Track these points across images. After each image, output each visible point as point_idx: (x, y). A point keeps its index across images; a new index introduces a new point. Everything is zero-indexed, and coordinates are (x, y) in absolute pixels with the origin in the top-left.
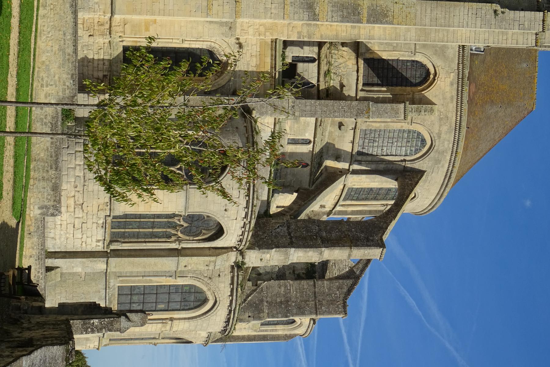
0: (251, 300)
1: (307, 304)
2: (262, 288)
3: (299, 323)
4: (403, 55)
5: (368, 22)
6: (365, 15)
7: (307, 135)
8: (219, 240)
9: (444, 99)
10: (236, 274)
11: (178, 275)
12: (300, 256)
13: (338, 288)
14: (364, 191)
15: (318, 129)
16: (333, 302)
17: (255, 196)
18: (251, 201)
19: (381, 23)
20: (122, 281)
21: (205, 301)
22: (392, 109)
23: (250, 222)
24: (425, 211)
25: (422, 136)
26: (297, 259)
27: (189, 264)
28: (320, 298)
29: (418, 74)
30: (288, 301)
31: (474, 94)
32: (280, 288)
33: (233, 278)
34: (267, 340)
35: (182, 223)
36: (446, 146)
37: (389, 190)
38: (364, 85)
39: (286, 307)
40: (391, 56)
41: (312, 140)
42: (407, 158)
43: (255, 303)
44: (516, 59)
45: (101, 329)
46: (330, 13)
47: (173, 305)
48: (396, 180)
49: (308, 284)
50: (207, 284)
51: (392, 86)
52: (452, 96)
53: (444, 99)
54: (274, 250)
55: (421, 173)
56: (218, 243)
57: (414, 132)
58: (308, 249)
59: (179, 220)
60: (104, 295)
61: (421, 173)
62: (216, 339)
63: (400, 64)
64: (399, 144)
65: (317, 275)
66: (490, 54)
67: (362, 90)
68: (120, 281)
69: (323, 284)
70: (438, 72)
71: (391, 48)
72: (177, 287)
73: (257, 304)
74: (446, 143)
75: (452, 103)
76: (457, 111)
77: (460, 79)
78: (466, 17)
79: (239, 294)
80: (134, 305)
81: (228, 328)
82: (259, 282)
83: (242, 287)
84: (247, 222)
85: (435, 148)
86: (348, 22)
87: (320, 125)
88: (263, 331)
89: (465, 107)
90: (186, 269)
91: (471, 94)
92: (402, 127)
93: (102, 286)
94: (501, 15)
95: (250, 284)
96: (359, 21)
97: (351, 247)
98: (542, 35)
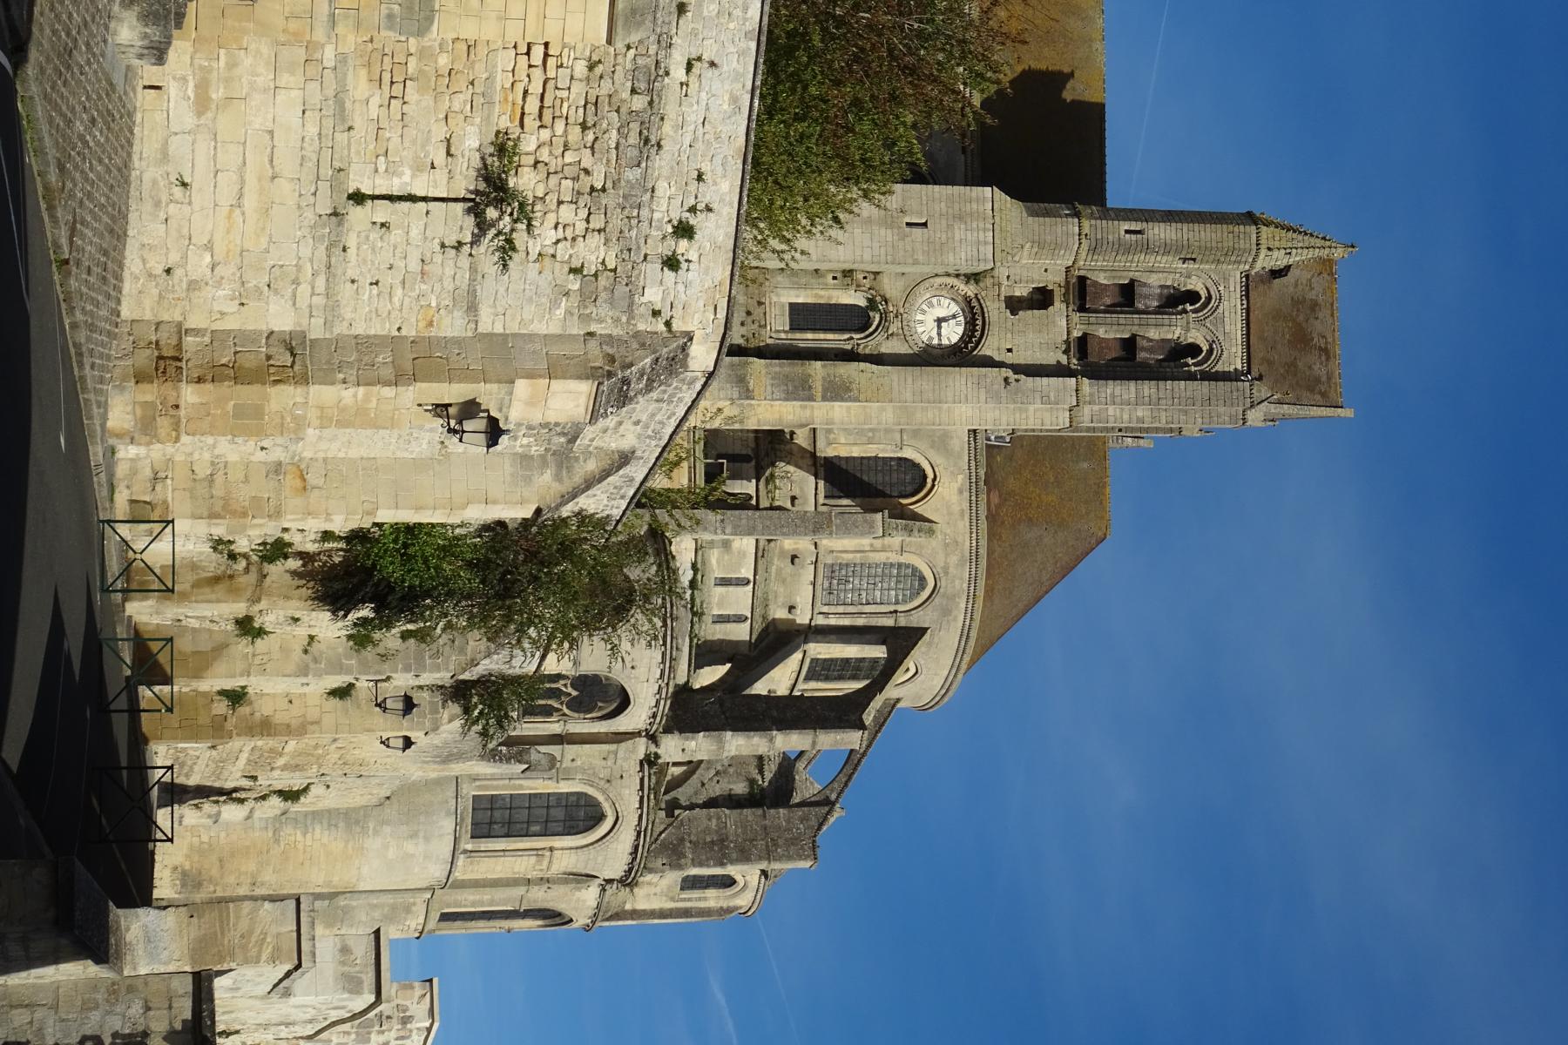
0: (665, 839)
1: (754, 846)
2: (682, 820)
3: (742, 884)
4: (883, 450)
5: (824, 399)
6: (820, 389)
7: (743, 571)
8: (622, 715)
9: (950, 514)
10: (646, 774)
11: (561, 776)
12: (741, 745)
13: (803, 819)
14: (835, 666)
15: (760, 562)
16: (793, 841)
17: (674, 645)
18: (668, 652)
19: (843, 400)
20: (480, 788)
21: (601, 817)
22: (866, 521)
23: (667, 684)
24: (937, 699)
25: (920, 572)
26: (737, 749)
27: (577, 756)
28: (775, 835)
29: (908, 478)
30: (722, 841)
31: (999, 506)
32: (709, 820)
33: (642, 780)
34: (692, 916)
35: (570, 690)
36: (958, 587)
37: (875, 661)
38: (826, 497)
39: (721, 849)
40: (865, 451)
41: (752, 578)
42: (900, 608)
43: (672, 843)
44: (1069, 455)
45: (510, 759)
46: (769, 388)
47: (553, 826)
48: (883, 643)
49: (754, 813)
50: (604, 792)
51: (869, 497)
52: (963, 510)
53: (950, 514)
54: (701, 734)
55: (922, 631)
56: (623, 723)
57: (907, 566)
58: (752, 733)
59: (565, 685)
60: (454, 807)
61: (922, 631)
62: (610, 914)
63: (880, 463)
64: (885, 585)
65: (767, 801)
66: (1022, 446)
67: (824, 505)
68: (479, 786)
69: (778, 813)
70: (938, 474)
71: (864, 439)
72: (559, 796)
73: (674, 845)
75: (963, 519)
76: (971, 533)
77: (973, 486)
78: (964, 387)
79: (651, 804)
80: (495, 826)
81: (635, 863)
82: (677, 812)
83: (655, 793)
84: (663, 685)
85: (942, 590)
86: (795, 400)
87: (763, 556)
88: (684, 900)
89: (984, 525)
90: (574, 764)
91: (993, 506)
92: (888, 558)
93: (451, 793)
94: (1014, 383)
95: (662, 814)
96: (811, 398)
97: (815, 729)
98: (1079, 411)
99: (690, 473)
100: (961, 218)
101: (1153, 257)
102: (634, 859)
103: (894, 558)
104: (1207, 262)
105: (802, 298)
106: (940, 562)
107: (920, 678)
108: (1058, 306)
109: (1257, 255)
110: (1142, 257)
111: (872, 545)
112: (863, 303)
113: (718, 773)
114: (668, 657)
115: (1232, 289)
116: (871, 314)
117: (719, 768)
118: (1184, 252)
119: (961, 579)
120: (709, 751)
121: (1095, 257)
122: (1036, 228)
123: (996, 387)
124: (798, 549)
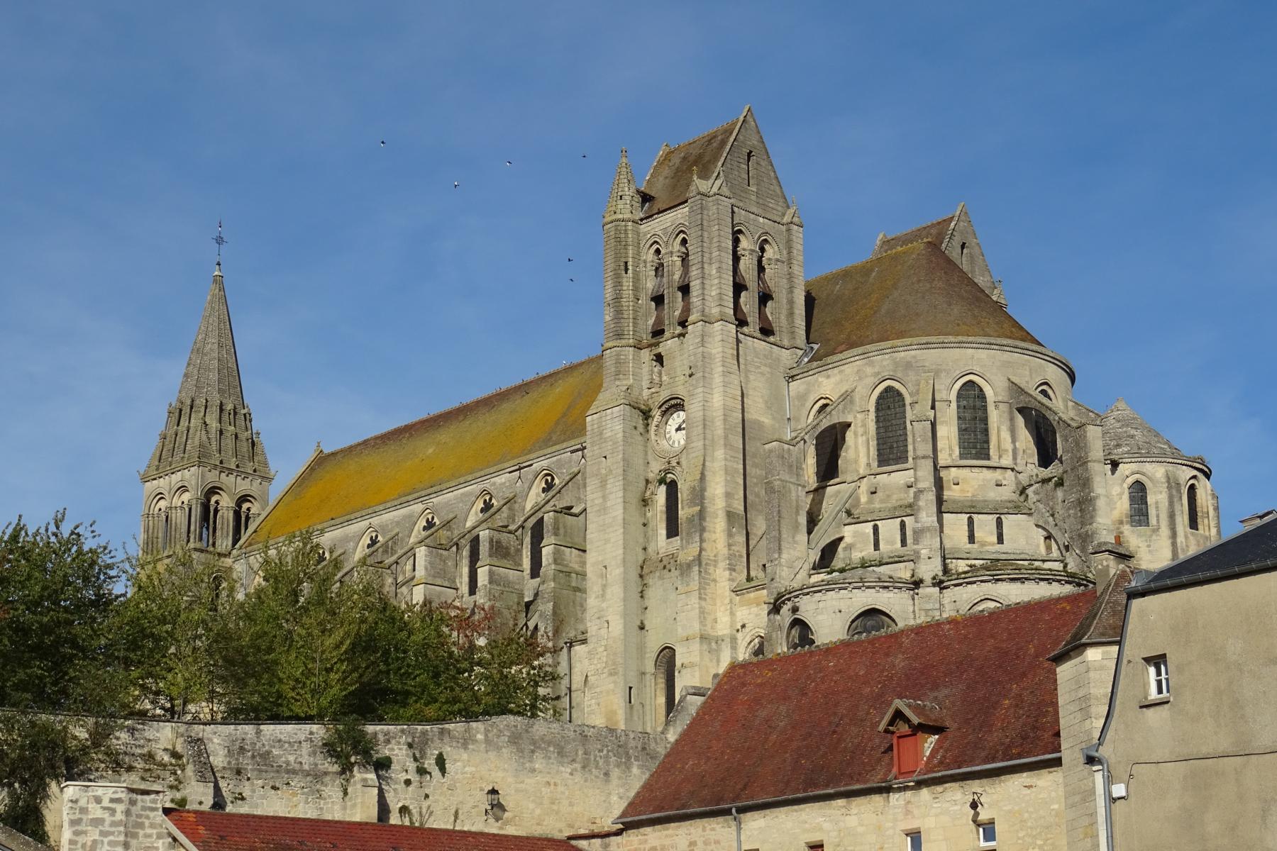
7: (867, 531)
9: (841, 381)
10: (949, 583)
12: (927, 514)
15: (861, 519)
16: (1077, 444)
18: (824, 587)
23: (850, 583)
33: (956, 585)
34: (1173, 511)
39: (1084, 503)
41: (872, 523)
46: (694, 545)
66: (828, 333)
74: (885, 363)
84: (852, 586)
85: (891, 373)
88: (1158, 521)
92: (872, 420)
99: (759, 589)
100: (601, 434)
101: (624, 292)
102: (1026, 579)
103: (872, 415)
104: (626, 253)
105: (663, 532)
106: (871, 381)
107: (977, 369)
108: (661, 349)
109: (618, 220)
110: (625, 300)
111: (862, 435)
112: (663, 488)
113: (1053, 515)
114: (827, 587)
115: (649, 228)
116: (668, 480)
117: (1048, 514)
118: (619, 272)
119: (882, 361)
120: (931, 537)
121: (626, 333)
122: (608, 380)
123: (694, 382)
124: (867, 491)
